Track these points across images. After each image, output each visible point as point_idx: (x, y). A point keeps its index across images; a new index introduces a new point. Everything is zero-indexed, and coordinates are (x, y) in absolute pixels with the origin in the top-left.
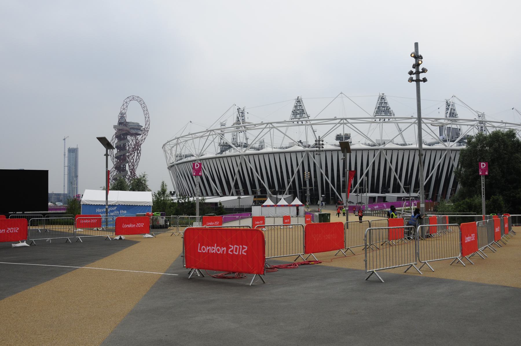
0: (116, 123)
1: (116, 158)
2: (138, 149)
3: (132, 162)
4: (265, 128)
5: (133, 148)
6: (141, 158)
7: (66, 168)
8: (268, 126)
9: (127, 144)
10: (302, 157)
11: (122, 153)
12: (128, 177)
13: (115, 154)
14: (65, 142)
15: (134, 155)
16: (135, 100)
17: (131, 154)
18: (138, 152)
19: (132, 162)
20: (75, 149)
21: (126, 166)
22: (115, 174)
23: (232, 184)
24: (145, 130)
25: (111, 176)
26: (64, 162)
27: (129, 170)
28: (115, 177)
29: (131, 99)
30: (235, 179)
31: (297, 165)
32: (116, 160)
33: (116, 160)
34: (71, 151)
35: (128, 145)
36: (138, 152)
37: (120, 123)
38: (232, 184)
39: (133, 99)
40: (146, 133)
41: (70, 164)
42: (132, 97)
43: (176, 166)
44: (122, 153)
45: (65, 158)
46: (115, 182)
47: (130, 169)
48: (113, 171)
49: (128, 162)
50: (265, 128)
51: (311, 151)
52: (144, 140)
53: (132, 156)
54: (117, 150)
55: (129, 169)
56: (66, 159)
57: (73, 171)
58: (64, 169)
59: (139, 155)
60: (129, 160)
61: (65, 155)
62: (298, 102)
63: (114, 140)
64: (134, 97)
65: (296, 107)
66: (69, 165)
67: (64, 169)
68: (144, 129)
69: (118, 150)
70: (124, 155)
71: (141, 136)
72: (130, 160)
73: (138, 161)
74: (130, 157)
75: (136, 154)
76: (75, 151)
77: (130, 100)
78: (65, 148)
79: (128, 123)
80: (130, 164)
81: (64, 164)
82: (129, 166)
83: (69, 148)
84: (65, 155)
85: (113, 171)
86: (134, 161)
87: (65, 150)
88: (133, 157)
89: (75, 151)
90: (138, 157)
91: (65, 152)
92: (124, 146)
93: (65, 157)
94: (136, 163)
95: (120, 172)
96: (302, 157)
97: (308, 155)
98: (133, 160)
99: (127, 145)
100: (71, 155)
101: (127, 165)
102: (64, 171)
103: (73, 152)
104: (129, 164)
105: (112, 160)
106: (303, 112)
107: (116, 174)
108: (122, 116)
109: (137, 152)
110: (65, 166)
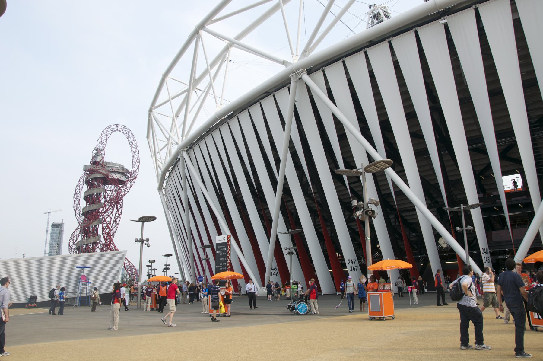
0: (88, 162)
1: (83, 215)
3: (108, 222)
7: (48, 246)
9: (102, 194)
11: (94, 207)
14: (49, 216)
15: (112, 212)
19: (108, 222)
20: (59, 224)
21: (97, 229)
22: (79, 239)
26: (46, 239)
27: (103, 234)
34: (55, 226)
35: (105, 197)
37: (95, 163)
39: (117, 130)
41: (53, 242)
44: (94, 207)
45: (47, 235)
47: (104, 232)
53: (110, 214)
55: (103, 232)
56: (49, 235)
57: (55, 249)
58: (45, 247)
60: (103, 220)
61: (47, 231)
66: (52, 242)
67: (45, 247)
69: (88, 204)
70: (97, 210)
76: (59, 226)
78: (48, 223)
79: (107, 163)
80: (105, 225)
81: (46, 242)
82: (103, 228)
83: (54, 223)
84: (47, 231)
86: (111, 221)
87: (48, 225)
89: (59, 226)
90: (117, 215)
91: (48, 228)
92: (98, 194)
93: (47, 233)
95: (89, 236)
98: (111, 219)
99: (102, 197)
100: (54, 231)
101: (100, 226)
102: (45, 249)
103: (57, 228)
105: (78, 219)
108: (98, 151)
109: (117, 207)
110: (46, 244)
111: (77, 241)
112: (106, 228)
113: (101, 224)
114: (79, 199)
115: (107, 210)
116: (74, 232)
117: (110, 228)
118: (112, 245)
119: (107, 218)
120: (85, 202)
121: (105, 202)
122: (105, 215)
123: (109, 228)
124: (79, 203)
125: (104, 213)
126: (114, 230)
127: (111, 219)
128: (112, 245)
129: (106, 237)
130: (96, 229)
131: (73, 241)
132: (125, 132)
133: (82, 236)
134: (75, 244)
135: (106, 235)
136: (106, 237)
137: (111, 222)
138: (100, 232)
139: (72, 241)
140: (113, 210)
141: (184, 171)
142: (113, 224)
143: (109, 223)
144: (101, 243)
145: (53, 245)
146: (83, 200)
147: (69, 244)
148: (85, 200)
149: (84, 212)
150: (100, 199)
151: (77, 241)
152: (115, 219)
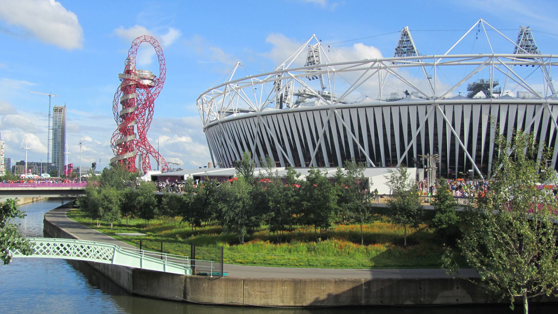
0: (122, 72)
1: (121, 117)
2: (150, 106)
4: (372, 68)
5: (143, 105)
6: (153, 117)
7: (51, 131)
8: (376, 65)
10: (426, 113)
12: (136, 142)
13: (120, 112)
16: (147, 41)
17: (140, 113)
18: (151, 109)
19: (141, 123)
22: (119, 138)
23: (313, 154)
24: (160, 82)
25: (115, 141)
27: (138, 133)
28: (119, 142)
29: (142, 40)
30: (317, 145)
31: (418, 126)
32: (121, 119)
33: (121, 119)
34: (57, 110)
36: (151, 109)
38: (313, 154)
39: (145, 41)
40: (161, 84)
42: (144, 37)
43: (221, 125)
46: (119, 149)
48: (117, 134)
50: (372, 68)
51: (440, 104)
52: (158, 94)
55: (138, 131)
59: (152, 113)
62: (405, 35)
63: (119, 93)
64: (146, 37)
65: (401, 42)
68: (158, 79)
71: (155, 88)
72: (139, 120)
73: (150, 121)
74: (140, 116)
75: (147, 112)
76: (62, 110)
77: (141, 42)
78: (50, 107)
84: (49, 115)
85: (117, 134)
86: (144, 121)
88: (143, 116)
89: (62, 110)
90: (149, 117)
94: (147, 124)
96: (426, 113)
97: (435, 109)
98: (144, 119)
104: (138, 126)
106: (411, 51)
107: (121, 137)
111: (118, 139)
120: (121, 106)
132: (152, 42)
138: (136, 131)
141: (220, 129)
145: (56, 130)
149: (121, 115)
152: (148, 120)
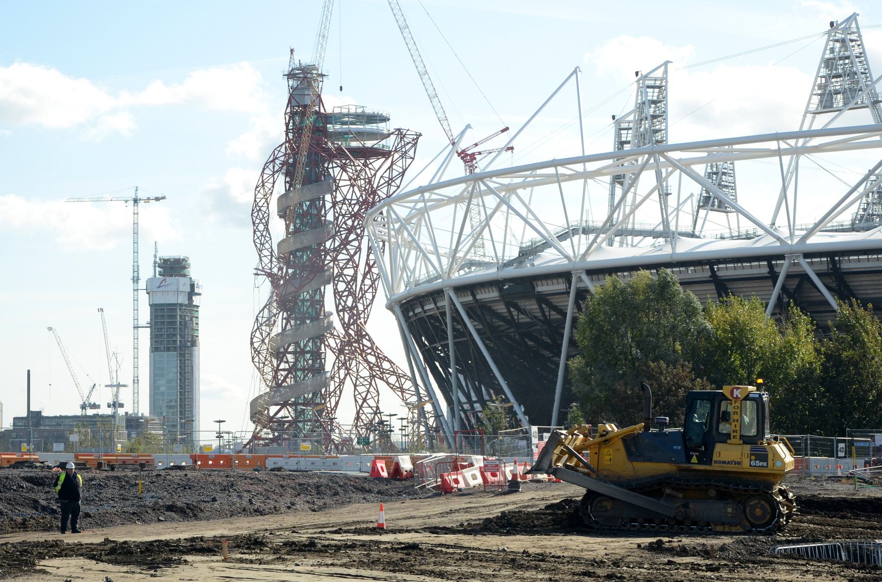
9: (328, 197)
13: (279, 245)
15: (359, 248)
19: (349, 278)
22: (277, 329)
25: (263, 341)
27: (338, 311)
47: (340, 307)
49: (332, 279)
52: (398, 182)
53: (352, 252)
54: (287, 227)
55: (337, 307)
60: (336, 271)
80: (341, 286)
86: (356, 273)
88: (355, 253)
98: (356, 267)
99: (328, 205)
101: (329, 289)
107: (284, 330)
111: (272, 335)
112: (346, 293)
113: (332, 284)
114: (266, 219)
115: (345, 243)
116: (263, 310)
117: (355, 295)
118: (364, 340)
119: (347, 263)
120: (282, 223)
121: (336, 219)
122: (341, 257)
123: (352, 293)
124: (267, 229)
125: (337, 250)
126: (369, 296)
127: (357, 266)
128: (364, 340)
129: (346, 320)
130: (317, 297)
131: (261, 334)
133: (283, 319)
134: (267, 341)
135: (347, 316)
136: (346, 320)
137: (356, 278)
138: (329, 304)
139: (258, 334)
140: (360, 244)
142: (363, 281)
143: (351, 280)
144: (335, 333)
146: (278, 217)
147: (252, 343)
148: (281, 217)
150: (323, 212)
151: (272, 335)
